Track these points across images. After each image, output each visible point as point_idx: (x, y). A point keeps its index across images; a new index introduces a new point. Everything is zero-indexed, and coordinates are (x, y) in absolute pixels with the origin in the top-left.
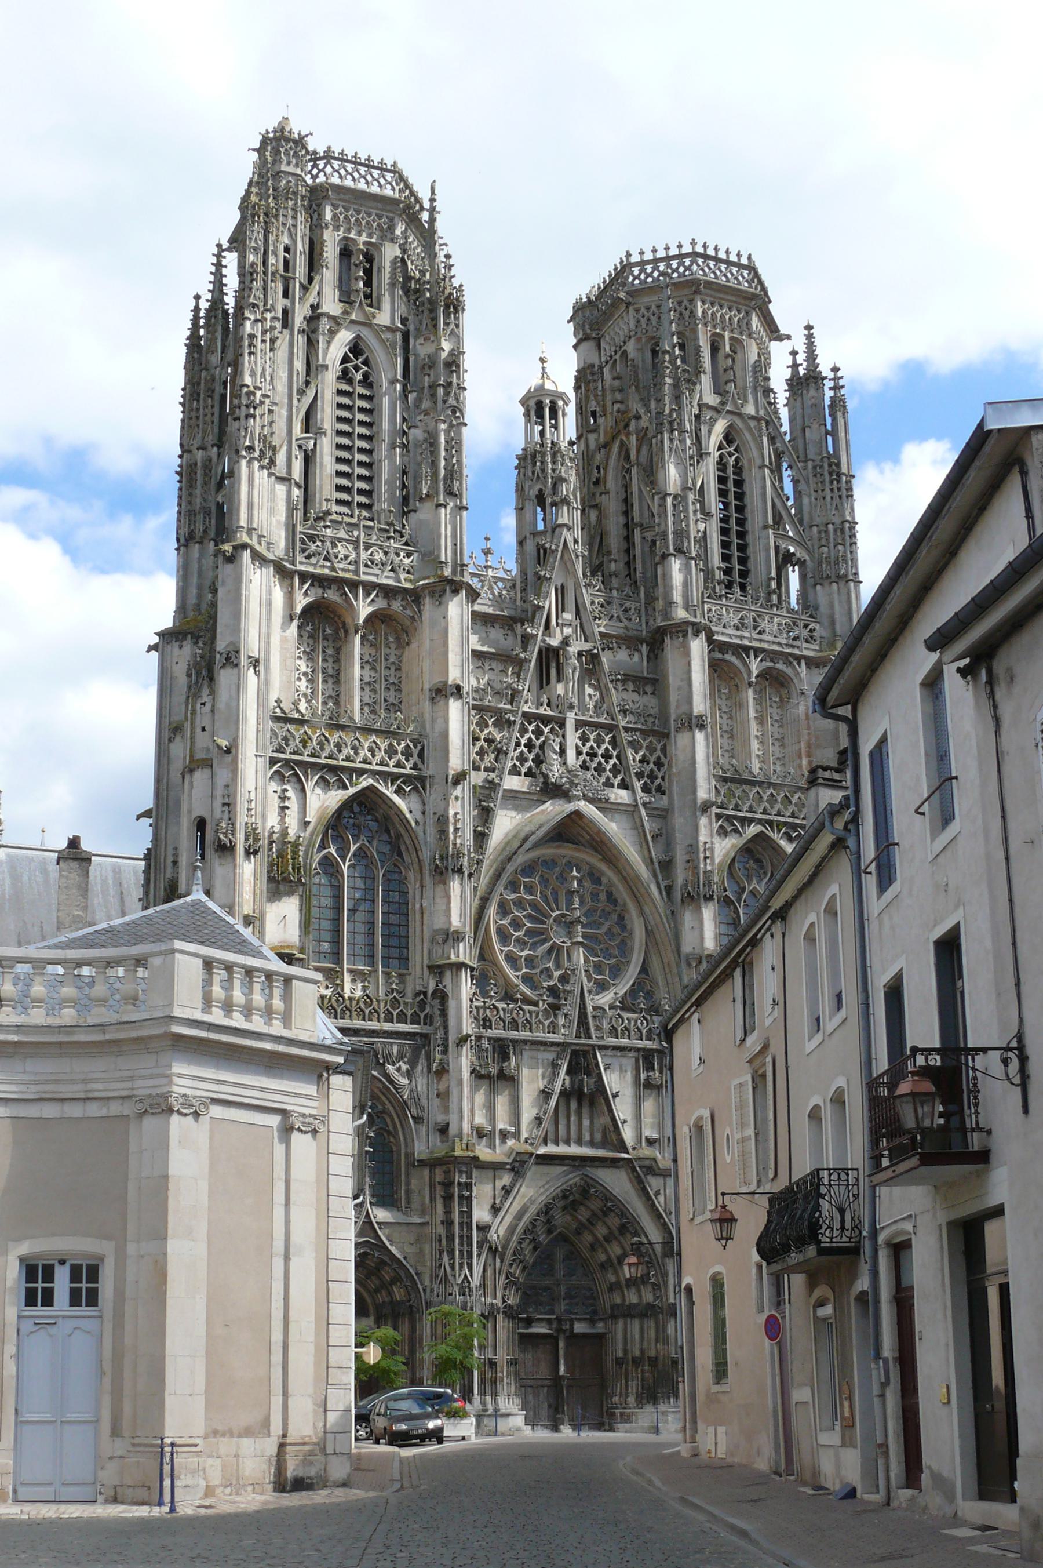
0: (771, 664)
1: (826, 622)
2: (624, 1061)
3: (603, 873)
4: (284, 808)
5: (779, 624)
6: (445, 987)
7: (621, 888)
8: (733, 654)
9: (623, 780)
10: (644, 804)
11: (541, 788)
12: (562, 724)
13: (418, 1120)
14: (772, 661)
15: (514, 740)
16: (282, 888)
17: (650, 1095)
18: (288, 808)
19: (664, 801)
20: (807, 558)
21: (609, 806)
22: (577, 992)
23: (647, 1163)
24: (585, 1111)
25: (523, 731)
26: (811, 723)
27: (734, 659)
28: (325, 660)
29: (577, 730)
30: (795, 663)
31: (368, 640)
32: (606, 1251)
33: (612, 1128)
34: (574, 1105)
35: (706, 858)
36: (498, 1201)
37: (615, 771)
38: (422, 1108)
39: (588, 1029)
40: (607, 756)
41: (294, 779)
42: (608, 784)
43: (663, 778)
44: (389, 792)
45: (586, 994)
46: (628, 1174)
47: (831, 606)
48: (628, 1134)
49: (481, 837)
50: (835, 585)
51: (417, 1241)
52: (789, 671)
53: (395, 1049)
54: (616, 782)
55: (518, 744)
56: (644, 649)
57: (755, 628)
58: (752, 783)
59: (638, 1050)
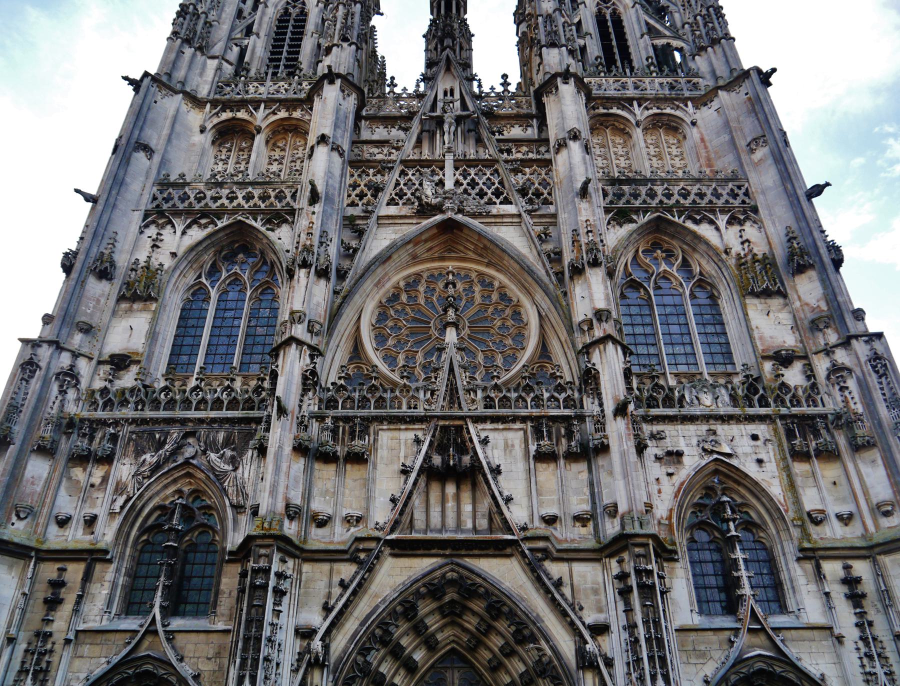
0: (659, 111)
1: (708, 76)
2: (510, 435)
3: (493, 278)
4: (155, 246)
5: (661, 84)
6: (277, 366)
7: (513, 287)
8: (618, 108)
9: (506, 198)
10: (529, 212)
11: (418, 211)
12: (442, 168)
13: (238, 508)
14: (658, 108)
15: (394, 181)
16: (135, 306)
17: (545, 470)
18: (158, 247)
19: (552, 209)
20: (683, 45)
21: (493, 220)
22: (446, 367)
23: (541, 544)
24: (466, 496)
25: (403, 173)
26: (708, 144)
27: (619, 112)
28: (237, 163)
29: (456, 169)
30: (681, 105)
31: (278, 147)
32: (508, 672)
33: (495, 509)
34: (451, 489)
35: (588, 232)
36: (332, 602)
37: (497, 194)
38: (246, 496)
39: (460, 404)
40: (489, 183)
41: (169, 227)
42: (490, 202)
43: (550, 194)
44: (258, 225)
45: (456, 369)
46: (519, 562)
47: (711, 64)
48: (517, 514)
49: (349, 253)
50: (709, 49)
51: (218, 655)
52: (678, 113)
53: (221, 436)
54: (498, 201)
55: (397, 184)
56: (535, 122)
57: (636, 88)
58: (645, 181)
59: (524, 419)
